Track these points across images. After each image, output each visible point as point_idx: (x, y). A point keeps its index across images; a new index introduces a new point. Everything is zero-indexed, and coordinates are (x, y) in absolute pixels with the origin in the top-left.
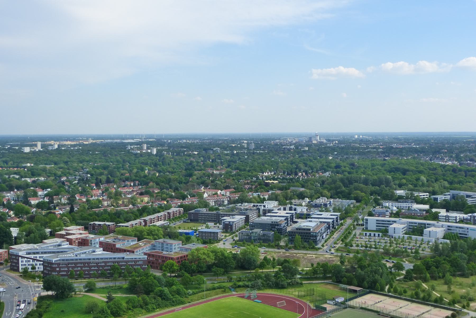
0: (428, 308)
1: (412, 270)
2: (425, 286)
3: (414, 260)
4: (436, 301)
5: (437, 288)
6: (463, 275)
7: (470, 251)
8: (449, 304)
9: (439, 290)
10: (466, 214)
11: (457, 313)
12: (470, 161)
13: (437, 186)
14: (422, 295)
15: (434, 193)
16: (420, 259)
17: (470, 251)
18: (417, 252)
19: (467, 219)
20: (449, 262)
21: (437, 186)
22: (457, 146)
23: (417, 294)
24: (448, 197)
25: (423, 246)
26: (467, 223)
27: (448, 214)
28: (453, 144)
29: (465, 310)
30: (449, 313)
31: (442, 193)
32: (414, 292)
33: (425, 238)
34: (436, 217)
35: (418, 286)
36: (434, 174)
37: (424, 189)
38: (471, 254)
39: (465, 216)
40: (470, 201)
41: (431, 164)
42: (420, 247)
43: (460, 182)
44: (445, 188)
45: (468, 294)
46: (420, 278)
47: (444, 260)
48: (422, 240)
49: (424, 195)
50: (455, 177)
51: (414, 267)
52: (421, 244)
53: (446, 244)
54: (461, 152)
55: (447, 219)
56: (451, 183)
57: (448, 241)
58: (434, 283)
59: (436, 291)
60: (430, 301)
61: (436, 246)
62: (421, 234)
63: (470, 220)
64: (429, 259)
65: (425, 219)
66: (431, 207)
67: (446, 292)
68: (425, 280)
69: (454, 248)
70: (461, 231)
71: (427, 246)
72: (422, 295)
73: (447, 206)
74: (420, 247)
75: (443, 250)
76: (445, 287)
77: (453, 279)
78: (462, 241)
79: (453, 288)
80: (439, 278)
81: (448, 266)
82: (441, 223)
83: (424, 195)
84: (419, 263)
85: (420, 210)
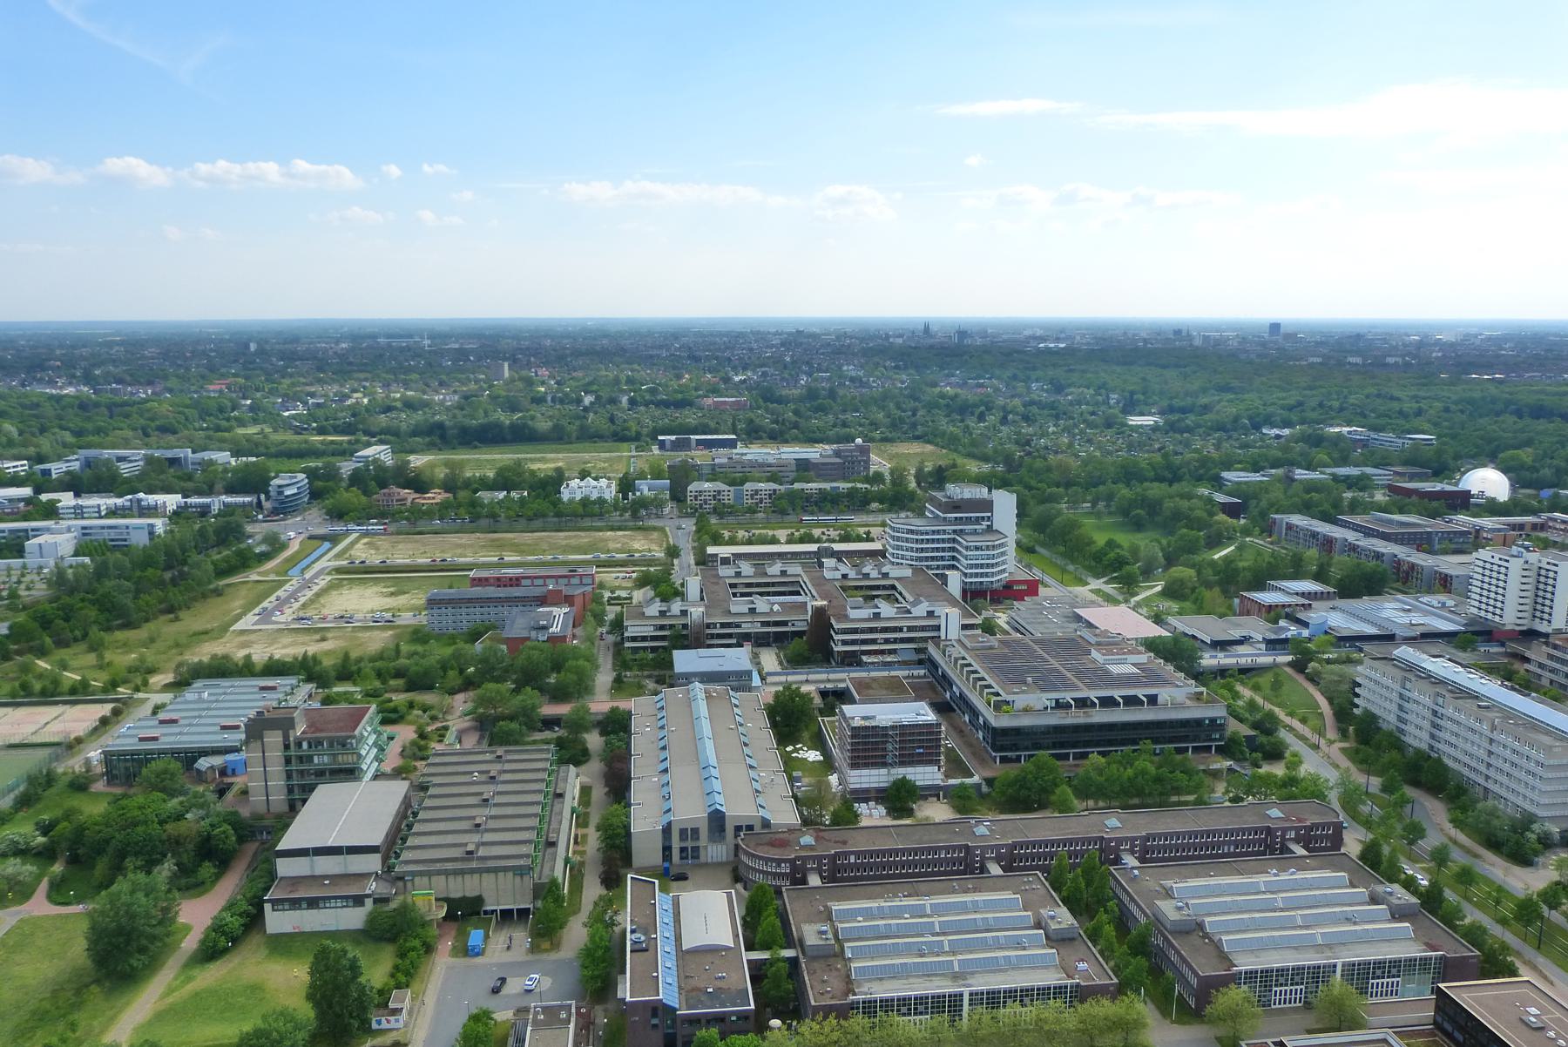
0: (53, 711)
1: (7, 637)
2: (42, 664)
3: (10, 614)
4: (73, 691)
5: (74, 663)
6: (128, 625)
7: (138, 573)
8: (105, 690)
9: (76, 666)
10: (120, 496)
11: (125, 704)
12: (118, 382)
13: (45, 444)
14: (37, 686)
15: (41, 459)
16: (25, 608)
17: (138, 573)
18: (13, 595)
19: (123, 508)
20: (93, 603)
21: (45, 444)
22: (84, 351)
23: (25, 687)
24: (76, 466)
25: (27, 579)
26: (124, 517)
27: (80, 502)
28: (73, 347)
29: (141, 695)
30: (106, 709)
31: (59, 458)
32: (17, 684)
33: (31, 561)
34: (51, 512)
35: (25, 669)
36: (35, 416)
37: (15, 451)
38: (140, 578)
39: (119, 501)
40: (125, 469)
41: (26, 395)
42: (19, 582)
43: (99, 431)
44: (65, 445)
45: (142, 660)
46: (31, 650)
47: (83, 600)
48: (24, 567)
49: (20, 467)
50: (85, 421)
51: (10, 628)
52: (23, 575)
53: (83, 565)
54: (95, 366)
55: (79, 512)
56: (78, 434)
57: (87, 560)
58: (63, 653)
59: (73, 671)
60: (60, 694)
61: (60, 573)
62: (20, 552)
63: (130, 509)
64: (47, 606)
65: (25, 518)
66: (38, 490)
67: (93, 667)
68: (42, 653)
69: (101, 573)
70: (113, 534)
71: (37, 578)
72: (37, 686)
73: (75, 484)
74: (19, 582)
75: (77, 580)
76: (91, 658)
77: (107, 637)
78: (118, 555)
79: (108, 656)
80: (76, 640)
81: (92, 613)
82: (64, 524)
83: (20, 467)
84: (21, 618)
85: (10, 500)
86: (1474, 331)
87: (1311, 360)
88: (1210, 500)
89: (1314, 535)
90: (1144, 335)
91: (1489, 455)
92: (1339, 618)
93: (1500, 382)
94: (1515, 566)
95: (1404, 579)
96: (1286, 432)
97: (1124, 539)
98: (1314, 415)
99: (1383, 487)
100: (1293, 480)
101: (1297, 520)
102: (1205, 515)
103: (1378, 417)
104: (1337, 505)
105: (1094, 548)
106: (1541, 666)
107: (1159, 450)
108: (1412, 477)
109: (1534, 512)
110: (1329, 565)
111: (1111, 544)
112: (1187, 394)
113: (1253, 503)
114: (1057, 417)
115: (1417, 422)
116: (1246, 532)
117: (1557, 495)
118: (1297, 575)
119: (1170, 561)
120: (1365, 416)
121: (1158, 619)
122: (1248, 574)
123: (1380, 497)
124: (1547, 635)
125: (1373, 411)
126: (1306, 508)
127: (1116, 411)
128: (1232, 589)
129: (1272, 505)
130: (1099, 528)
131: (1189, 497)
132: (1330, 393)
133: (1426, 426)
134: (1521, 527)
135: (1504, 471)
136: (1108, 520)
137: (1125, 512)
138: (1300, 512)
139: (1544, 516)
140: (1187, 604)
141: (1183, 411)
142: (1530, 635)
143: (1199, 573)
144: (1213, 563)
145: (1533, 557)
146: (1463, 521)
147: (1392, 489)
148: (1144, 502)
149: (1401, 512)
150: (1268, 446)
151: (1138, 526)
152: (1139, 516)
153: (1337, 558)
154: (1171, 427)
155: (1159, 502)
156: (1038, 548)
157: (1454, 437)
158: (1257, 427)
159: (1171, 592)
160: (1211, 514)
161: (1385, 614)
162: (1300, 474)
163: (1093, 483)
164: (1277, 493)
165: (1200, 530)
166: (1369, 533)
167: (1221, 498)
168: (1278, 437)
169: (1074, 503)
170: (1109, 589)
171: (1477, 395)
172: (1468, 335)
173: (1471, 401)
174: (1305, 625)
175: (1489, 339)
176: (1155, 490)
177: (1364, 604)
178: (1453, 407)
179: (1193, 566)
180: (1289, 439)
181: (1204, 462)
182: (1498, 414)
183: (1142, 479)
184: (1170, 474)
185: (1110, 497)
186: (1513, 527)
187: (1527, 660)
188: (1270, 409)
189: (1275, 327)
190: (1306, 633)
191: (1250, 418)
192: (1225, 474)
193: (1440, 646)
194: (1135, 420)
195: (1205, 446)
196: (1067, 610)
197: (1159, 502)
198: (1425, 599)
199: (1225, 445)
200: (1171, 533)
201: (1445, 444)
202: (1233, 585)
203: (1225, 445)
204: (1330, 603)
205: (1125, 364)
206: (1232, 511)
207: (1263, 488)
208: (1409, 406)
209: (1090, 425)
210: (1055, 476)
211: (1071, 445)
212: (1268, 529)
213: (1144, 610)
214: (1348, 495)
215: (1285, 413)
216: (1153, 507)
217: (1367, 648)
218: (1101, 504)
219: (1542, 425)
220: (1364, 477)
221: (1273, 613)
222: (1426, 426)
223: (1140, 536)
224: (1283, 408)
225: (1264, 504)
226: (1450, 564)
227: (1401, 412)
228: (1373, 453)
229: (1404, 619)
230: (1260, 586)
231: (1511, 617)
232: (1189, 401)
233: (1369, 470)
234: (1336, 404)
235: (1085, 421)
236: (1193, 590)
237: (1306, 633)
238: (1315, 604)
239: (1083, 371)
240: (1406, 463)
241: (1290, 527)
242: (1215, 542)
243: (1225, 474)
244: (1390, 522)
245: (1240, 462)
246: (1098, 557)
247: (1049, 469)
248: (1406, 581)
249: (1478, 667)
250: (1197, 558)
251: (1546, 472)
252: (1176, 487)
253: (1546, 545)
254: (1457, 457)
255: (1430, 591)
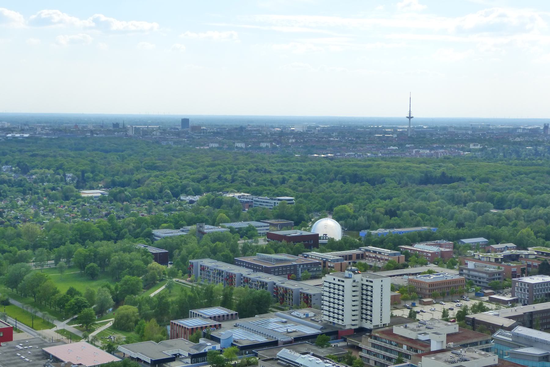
86: (313, 124)
87: (211, 145)
88: (146, 252)
89: (220, 273)
90: (90, 127)
91: (327, 209)
92: (240, 332)
93: (332, 159)
94: (348, 283)
95: (281, 300)
96: (197, 198)
97: (82, 287)
98: (215, 185)
99: (263, 234)
100: (203, 233)
101: (208, 263)
102: (141, 263)
103: (258, 185)
104: (234, 250)
105: (57, 297)
106: (369, 352)
107: (106, 215)
108: (282, 227)
109: (357, 247)
110: (231, 294)
111: (72, 292)
112: (125, 172)
113: (176, 252)
114: (24, 193)
115: (282, 188)
116: (173, 274)
117: (369, 235)
118: (209, 305)
119: (118, 301)
120: (249, 185)
121: (110, 349)
122: (176, 307)
123: (262, 242)
124: (370, 331)
125: (254, 181)
126: (213, 254)
127: (72, 187)
128: (166, 318)
129: (190, 253)
130: (62, 280)
131: (130, 251)
132: (225, 169)
133: (288, 191)
134: (350, 257)
135: (338, 220)
136: (67, 273)
137: (81, 266)
138: (209, 257)
139: (363, 248)
140: (132, 334)
141: (123, 185)
142: (361, 331)
143: (140, 308)
144: (149, 301)
145: (358, 277)
146: (315, 255)
147: (270, 236)
148: (95, 257)
149: (276, 252)
150: (185, 209)
151: (92, 276)
152: (90, 268)
153: (236, 289)
154: (115, 198)
155: (107, 256)
156: (11, 301)
157: (306, 197)
158: (176, 195)
159: (121, 326)
160: (147, 263)
161: (271, 326)
162: (208, 228)
163: (54, 244)
164: (193, 244)
165: (139, 276)
166: (256, 268)
167: (153, 250)
168: (191, 202)
169: (40, 261)
170: (71, 328)
171: (318, 168)
172: (309, 127)
173: (315, 173)
174: (217, 340)
175: (323, 129)
176: (104, 247)
177: (257, 319)
178: (304, 177)
179: (134, 304)
180: (201, 203)
181: (139, 223)
182: (331, 181)
183: (94, 239)
184: (115, 234)
185: (69, 255)
186: (346, 258)
187: (360, 349)
188: (185, 182)
189: (185, 121)
190: (218, 347)
191: (171, 189)
192: (155, 232)
193: (307, 346)
194: (86, 193)
195: (140, 211)
196: (37, 350)
197: (107, 256)
198: (295, 313)
199: (155, 209)
200: (118, 280)
201: (300, 202)
202: (164, 315)
203: (155, 209)
204: (234, 323)
205: (76, 149)
206: (162, 259)
207: (183, 241)
208: (276, 177)
209: (53, 198)
210: (24, 241)
211: (36, 215)
212: (188, 271)
213: (99, 343)
214: (241, 242)
215: (196, 185)
216: (103, 260)
217: (260, 353)
218: (63, 261)
219: (357, 187)
220: (251, 228)
221: (194, 334)
222: (288, 191)
223: (94, 283)
224: (193, 180)
225: (184, 252)
226: (309, 286)
227: (272, 181)
228: (255, 211)
229: (282, 329)
230: (185, 315)
231: (348, 320)
232: (127, 177)
233: (254, 223)
234: (229, 177)
235: (47, 195)
236: (136, 322)
237: (218, 347)
238: (223, 324)
239: (44, 156)
240: (278, 217)
241: (203, 268)
242: (151, 284)
243: (155, 232)
244: (270, 260)
245: (166, 222)
246: (61, 303)
247: (19, 235)
248: (282, 301)
249: (331, 358)
250: (137, 297)
251: (362, 219)
252: (119, 243)
253: (366, 268)
254: (309, 211)
255: (298, 307)
